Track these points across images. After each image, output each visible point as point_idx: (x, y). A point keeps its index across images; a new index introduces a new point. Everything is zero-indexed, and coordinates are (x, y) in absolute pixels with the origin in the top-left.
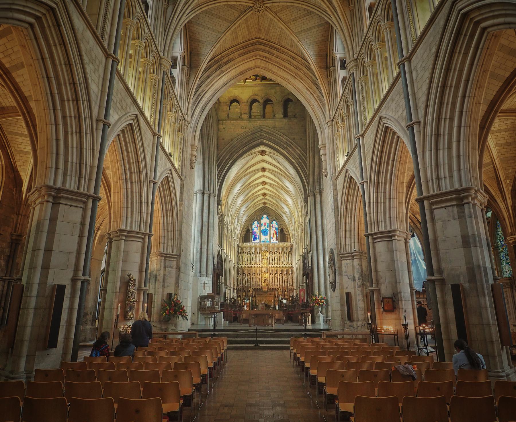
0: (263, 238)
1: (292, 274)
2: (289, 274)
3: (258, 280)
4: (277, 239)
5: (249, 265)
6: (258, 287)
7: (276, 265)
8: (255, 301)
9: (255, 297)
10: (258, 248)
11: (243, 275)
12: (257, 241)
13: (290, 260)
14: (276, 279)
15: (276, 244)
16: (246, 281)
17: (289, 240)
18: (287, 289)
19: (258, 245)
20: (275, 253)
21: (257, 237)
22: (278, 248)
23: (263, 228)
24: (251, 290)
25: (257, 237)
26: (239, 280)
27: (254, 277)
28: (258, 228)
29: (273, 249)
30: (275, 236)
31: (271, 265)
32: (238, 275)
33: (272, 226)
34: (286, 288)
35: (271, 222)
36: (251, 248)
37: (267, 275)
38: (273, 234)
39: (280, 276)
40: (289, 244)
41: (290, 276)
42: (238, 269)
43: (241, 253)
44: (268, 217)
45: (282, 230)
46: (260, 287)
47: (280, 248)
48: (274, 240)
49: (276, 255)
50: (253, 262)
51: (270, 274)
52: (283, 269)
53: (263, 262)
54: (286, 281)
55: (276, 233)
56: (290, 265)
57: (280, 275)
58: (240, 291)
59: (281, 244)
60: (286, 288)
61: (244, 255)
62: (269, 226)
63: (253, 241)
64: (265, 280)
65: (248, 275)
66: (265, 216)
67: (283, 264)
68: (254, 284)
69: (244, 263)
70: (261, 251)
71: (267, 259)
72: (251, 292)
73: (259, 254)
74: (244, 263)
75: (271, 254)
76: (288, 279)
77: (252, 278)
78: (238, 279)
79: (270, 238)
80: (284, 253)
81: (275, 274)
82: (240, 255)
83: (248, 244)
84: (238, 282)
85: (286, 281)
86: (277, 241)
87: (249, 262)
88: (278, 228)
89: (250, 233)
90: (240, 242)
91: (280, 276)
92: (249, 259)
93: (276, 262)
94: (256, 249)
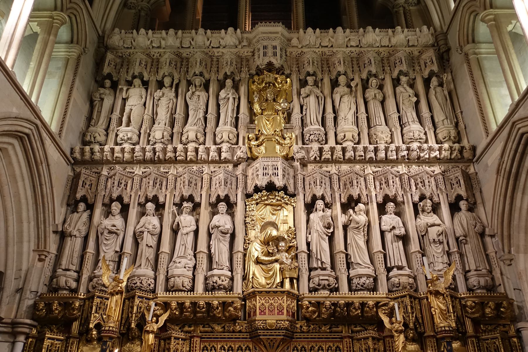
11: (108, 213)
16: (120, 255)
41: (463, 216)
51: (310, 207)
77: (175, 231)
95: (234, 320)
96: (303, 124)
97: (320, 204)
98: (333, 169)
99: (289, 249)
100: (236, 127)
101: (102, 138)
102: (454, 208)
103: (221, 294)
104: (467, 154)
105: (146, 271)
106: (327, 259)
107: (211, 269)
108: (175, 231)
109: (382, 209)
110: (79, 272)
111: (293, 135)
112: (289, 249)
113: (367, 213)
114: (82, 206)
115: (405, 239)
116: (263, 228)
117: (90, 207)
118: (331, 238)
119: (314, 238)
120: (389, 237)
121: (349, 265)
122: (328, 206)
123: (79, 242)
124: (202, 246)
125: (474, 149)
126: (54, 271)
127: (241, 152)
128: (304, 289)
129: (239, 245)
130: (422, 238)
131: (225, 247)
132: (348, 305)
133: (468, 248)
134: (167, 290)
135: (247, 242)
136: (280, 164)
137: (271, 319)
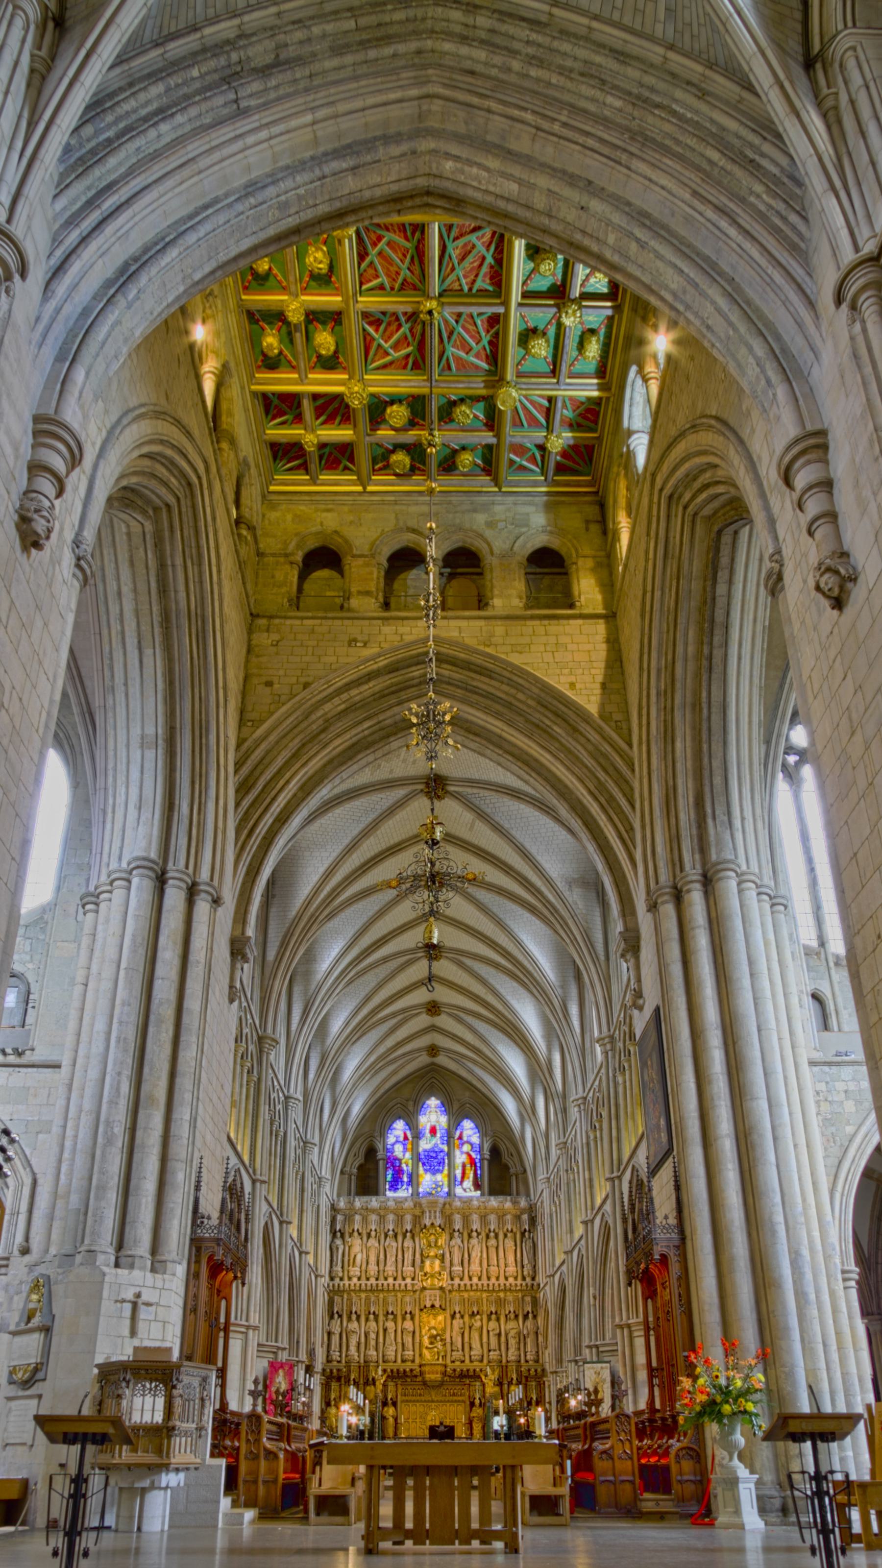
0: (426, 1180)
1: (535, 1317)
2: (526, 1317)
3: (408, 1339)
4: (477, 1186)
5: (373, 1281)
6: (408, 1366)
7: (475, 1280)
8: (396, 1419)
9: (394, 1404)
10: (408, 1218)
11: (349, 1319)
12: (403, 1193)
13: (526, 1261)
14: (475, 1335)
15: (475, 1203)
16: (359, 1344)
17: (522, 1189)
18: (519, 1374)
19: (409, 1204)
20: (470, 1236)
21: (405, 1179)
22: (483, 1218)
23: (425, 1145)
24: (379, 1375)
25: (405, 1179)
26: (335, 1339)
27: (390, 1325)
28: (409, 1146)
29: (466, 1219)
30: (470, 1174)
31: (457, 1281)
32: (331, 1317)
33: (460, 1138)
34: (513, 1368)
35: (455, 1122)
36: (382, 1219)
37: (440, 1318)
38: (464, 1166)
39: (493, 1324)
40: (523, 1203)
41: (529, 1322)
42: (334, 1293)
43: (342, 1236)
44: (448, 1106)
45: (495, 1151)
46: (415, 1366)
47: (492, 1218)
48: (466, 1190)
49: (474, 1241)
50: (390, 1269)
51: (453, 1317)
52: (502, 1295)
53: (427, 1268)
54: (512, 1342)
55: (473, 1162)
56: (528, 1280)
57: (489, 1319)
58: (339, 1379)
59: (494, 1202)
60: (513, 1368)
61: (356, 1244)
62: (449, 1137)
63: (389, 1194)
64: (435, 1337)
65: (367, 1320)
66: (433, 1102)
67: (502, 1278)
68: (391, 1353)
69: (355, 1271)
70: (419, 1227)
71: (442, 1261)
72: (379, 1387)
73: (413, 1237)
74: (355, 1271)
75: (457, 1241)
76: (519, 1333)
77: (385, 1330)
78: (329, 1334)
79: (451, 1177)
80: (505, 1236)
81: (473, 1315)
82: (339, 1242)
83: (374, 1202)
84: (329, 1345)
85: (512, 1342)
86: (478, 1193)
87: (373, 1269)
88: (481, 1147)
89: (377, 1163)
90: (339, 1195)
91: (493, 1324)
92: (373, 1259)
93: (475, 1267)
94: (400, 1219)
95: (416, 1376)
96: (451, 1264)
97: (458, 1316)
98: (466, 1295)
99: (442, 1340)
100: (413, 1266)
101: (340, 1274)
102: (526, 1317)
103: (409, 1364)
104: (535, 1288)
105: (372, 1353)
106: (460, 1346)
107: (403, 1350)
108: (385, 1330)
109: (489, 1319)
110: (340, 1351)
111: (445, 1274)
112: (442, 1340)
113: (481, 1320)
114: (336, 1316)
115: (499, 1335)
116: (430, 1329)
117: (340, 1316)
118: (463, 1334)
119: (454, 1334)
120: (491, 1333)
121: (471, 1348)
122: (462, 1317)
123: (338, 1336)
124: (399, 1340)
125: (539, 1285)
126: (328, 1352)
127: (419, 1285)
128: (448, 1362)
129: (417, 1340)
130: (507, 1335)
131: (410, 1339)
132: (468, 1370)
133: (529, 1340)
134: (384, 1362)
135: (421, 1336)
136: (438, 1293)
137: (433, 1377)
